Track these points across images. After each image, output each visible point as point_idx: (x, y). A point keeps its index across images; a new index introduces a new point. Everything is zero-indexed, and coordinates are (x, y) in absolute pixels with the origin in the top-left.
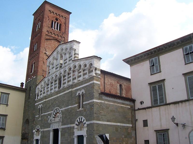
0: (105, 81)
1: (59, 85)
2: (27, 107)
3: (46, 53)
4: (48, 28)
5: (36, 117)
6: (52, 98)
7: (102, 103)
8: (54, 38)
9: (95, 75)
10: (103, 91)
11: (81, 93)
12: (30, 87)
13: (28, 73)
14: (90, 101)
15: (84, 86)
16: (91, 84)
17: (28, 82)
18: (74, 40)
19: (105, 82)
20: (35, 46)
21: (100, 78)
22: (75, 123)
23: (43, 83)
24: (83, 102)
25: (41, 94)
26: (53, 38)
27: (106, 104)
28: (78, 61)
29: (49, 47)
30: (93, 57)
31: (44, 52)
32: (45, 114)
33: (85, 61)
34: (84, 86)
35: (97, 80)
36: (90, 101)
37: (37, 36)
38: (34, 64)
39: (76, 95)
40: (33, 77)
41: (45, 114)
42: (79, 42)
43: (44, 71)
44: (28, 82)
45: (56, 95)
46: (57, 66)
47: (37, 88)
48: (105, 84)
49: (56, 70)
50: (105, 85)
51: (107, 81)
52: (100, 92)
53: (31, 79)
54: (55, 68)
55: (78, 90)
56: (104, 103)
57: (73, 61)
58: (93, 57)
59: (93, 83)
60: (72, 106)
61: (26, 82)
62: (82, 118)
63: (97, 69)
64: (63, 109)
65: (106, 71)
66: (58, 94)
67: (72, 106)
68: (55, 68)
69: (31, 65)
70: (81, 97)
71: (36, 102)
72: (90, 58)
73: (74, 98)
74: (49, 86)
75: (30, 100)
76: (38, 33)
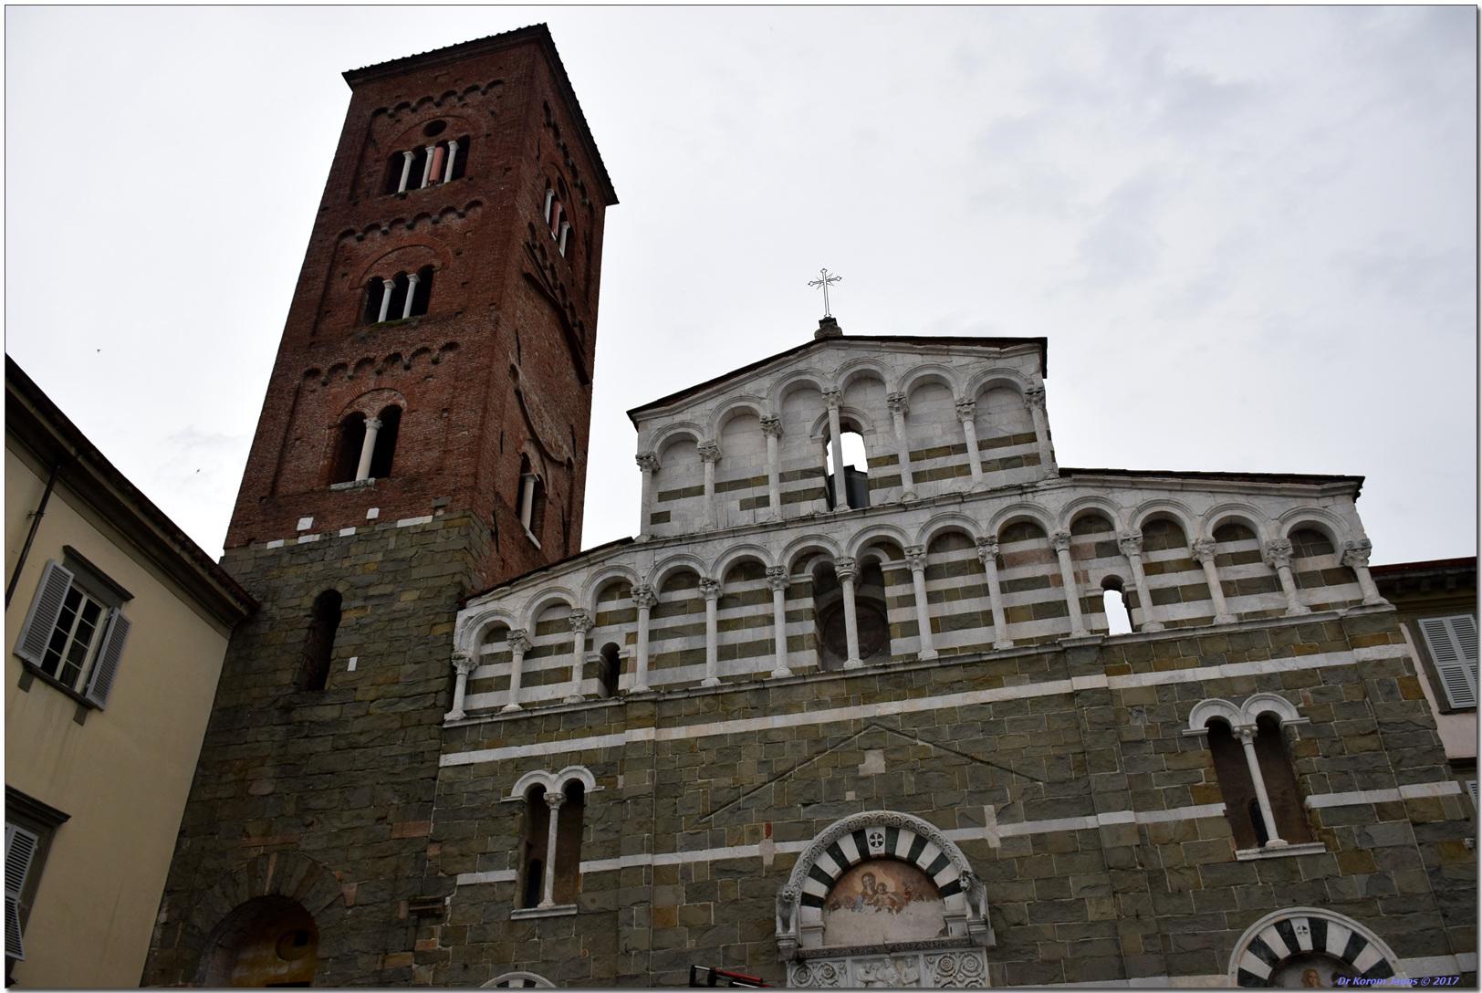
2: (269, 770)
4: (536, 209)
5: (463, 879)
6: (778, 721)
13: (269, 471)
15: (1269, 667)
22: (1233, 967)
23: (585, 586)
29: (530, 340)
30: (1340, 484)
31: (513, 360)
32: (663, 860)
33: (1241, 500)
34: (1269, 667)
37: (428, 222)
39: (1186, 733)
41: (663, 860)
47: (462, 616)
55: (1195, 691)
58: (1334, 489)
60: (1145, 818)
62: (1318, 929)
64: (995, 832)
67: (1145, 818)
71: (453, 738)
72: (1319, 487)
75: (328, 713)
76: (450, 209)
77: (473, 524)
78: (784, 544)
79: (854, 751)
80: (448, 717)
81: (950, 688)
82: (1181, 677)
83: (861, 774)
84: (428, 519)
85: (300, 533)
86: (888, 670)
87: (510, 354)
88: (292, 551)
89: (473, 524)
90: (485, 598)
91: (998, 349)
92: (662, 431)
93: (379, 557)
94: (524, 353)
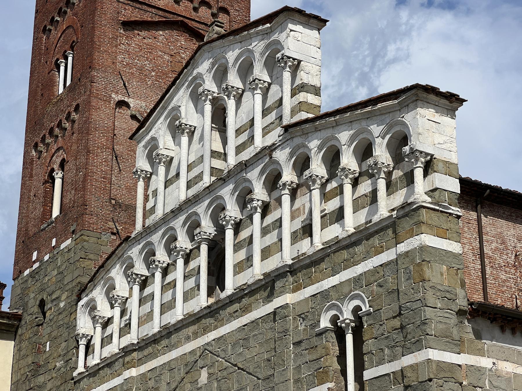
0: (485, 244)
1: (214, 278)
3: (127, 105)
7: (479, 370)
8: (167, 15)
9: (429, 200)
10: (478, 298)
11: (347, 315)
12: (42, 304)
14: (408, 360)
16: (407, 252)
17: (27, 272)
18: (286, 9)
19: (486, 251)
20: (62, 69)
21: (458, 217)
24: (359, 368)
25: (106, 341)
26: (160, 13)
27: (509, 380)
28: (317, 130)
29: (141, 69)
35: (442, 234)
36: (408, 360)
38: (62, 166)
40: (58, 244)
42: (316, 18)
43: (118, 206)
44: (27, 272)
45: (196, 335)
46: (195, 172)
48: (487, 261)
49: (192, 192)
50: (488, 270)
51: (494, 245)
52: (462, 303)
53: (46, 258)
54: (183, 182)
56: (494, 374)
57: (287, 128)
59: (423, 248)
61: (17, 274)
63: (441, 166)
65: (487, 187)
66: (206, 330)
68: (183, 182)
69: (40, 174)
70: (349, 339)
73: (304, 345)
74: (156, 287)
75: (41, 379)
77: (87, 238)
78: (182, 222)
79: (197, 370)
80: (75, 374)
81: (234, 316)
82: (322, 287)
83: (199, 386)
84: (69, 242)
85: (34, 262)
86: (212, 309)
87: (113, 96)
88: (32, 275)
89: (87, 238)
90: (87, 291)
91: (268, 25)
92: (145, 147)
93: (55, 272)
94: (134, 85)
